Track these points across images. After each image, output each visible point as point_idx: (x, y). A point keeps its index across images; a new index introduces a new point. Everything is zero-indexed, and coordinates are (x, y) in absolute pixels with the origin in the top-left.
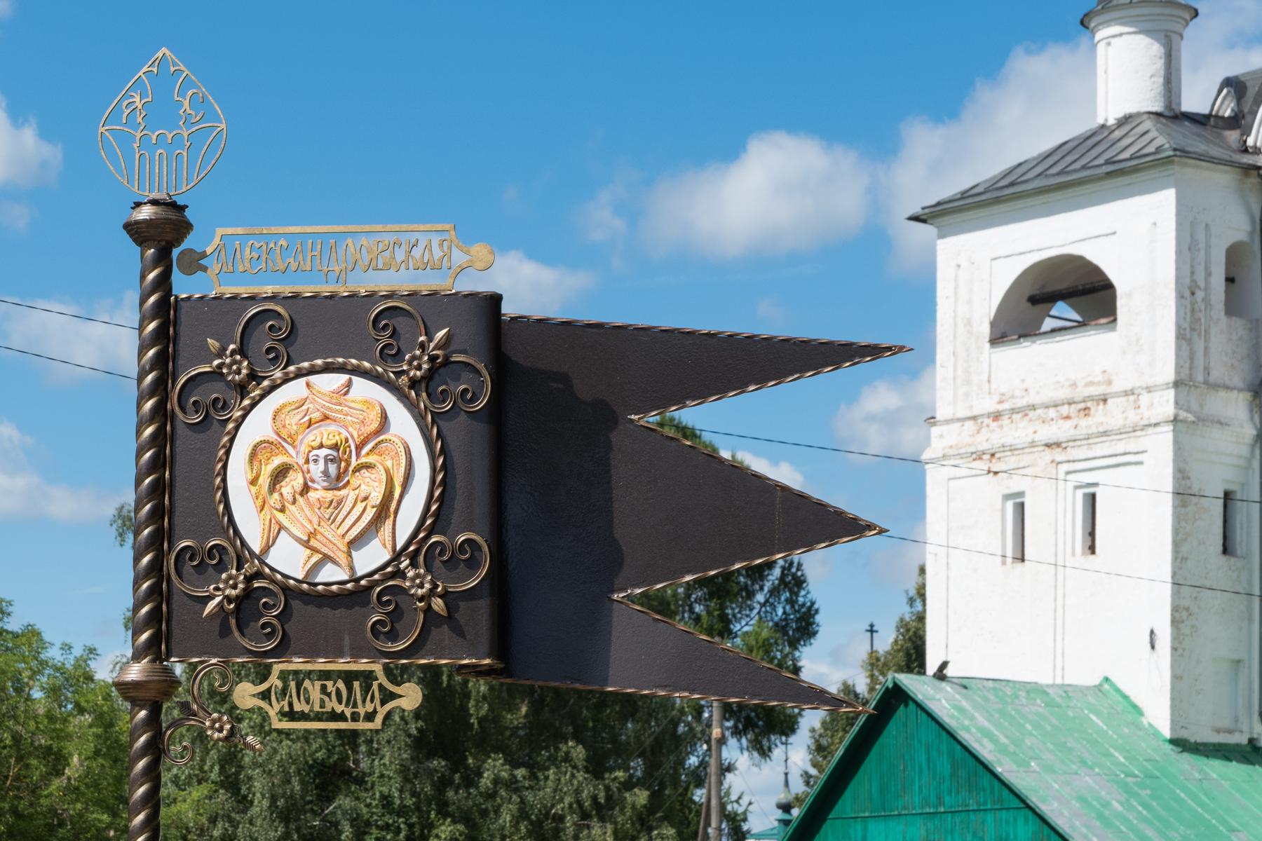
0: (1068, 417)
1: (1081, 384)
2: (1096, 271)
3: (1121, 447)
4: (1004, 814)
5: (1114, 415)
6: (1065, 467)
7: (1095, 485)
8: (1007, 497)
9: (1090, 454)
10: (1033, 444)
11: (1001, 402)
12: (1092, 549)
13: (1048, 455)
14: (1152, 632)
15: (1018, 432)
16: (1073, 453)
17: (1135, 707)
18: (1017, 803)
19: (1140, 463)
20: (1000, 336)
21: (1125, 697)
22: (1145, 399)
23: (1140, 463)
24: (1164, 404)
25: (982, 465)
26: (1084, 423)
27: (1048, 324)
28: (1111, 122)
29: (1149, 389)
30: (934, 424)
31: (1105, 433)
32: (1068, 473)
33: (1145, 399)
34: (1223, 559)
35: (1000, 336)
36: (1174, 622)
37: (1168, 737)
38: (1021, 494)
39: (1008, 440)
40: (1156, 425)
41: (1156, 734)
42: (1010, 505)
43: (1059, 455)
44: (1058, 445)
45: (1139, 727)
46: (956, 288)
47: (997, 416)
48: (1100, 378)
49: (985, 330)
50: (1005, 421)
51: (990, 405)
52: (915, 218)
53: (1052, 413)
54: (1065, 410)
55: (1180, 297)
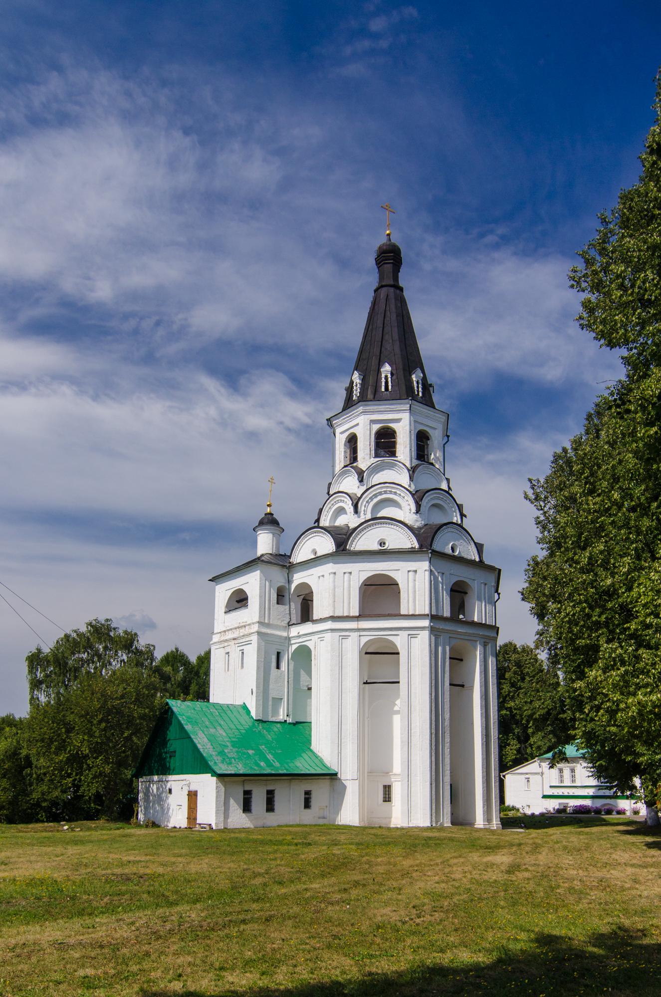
3: (247, 639)
7: (243, 650)
12: (242, 667)
13: (233, 642)
36: (257, 687)
43: (236, 642)
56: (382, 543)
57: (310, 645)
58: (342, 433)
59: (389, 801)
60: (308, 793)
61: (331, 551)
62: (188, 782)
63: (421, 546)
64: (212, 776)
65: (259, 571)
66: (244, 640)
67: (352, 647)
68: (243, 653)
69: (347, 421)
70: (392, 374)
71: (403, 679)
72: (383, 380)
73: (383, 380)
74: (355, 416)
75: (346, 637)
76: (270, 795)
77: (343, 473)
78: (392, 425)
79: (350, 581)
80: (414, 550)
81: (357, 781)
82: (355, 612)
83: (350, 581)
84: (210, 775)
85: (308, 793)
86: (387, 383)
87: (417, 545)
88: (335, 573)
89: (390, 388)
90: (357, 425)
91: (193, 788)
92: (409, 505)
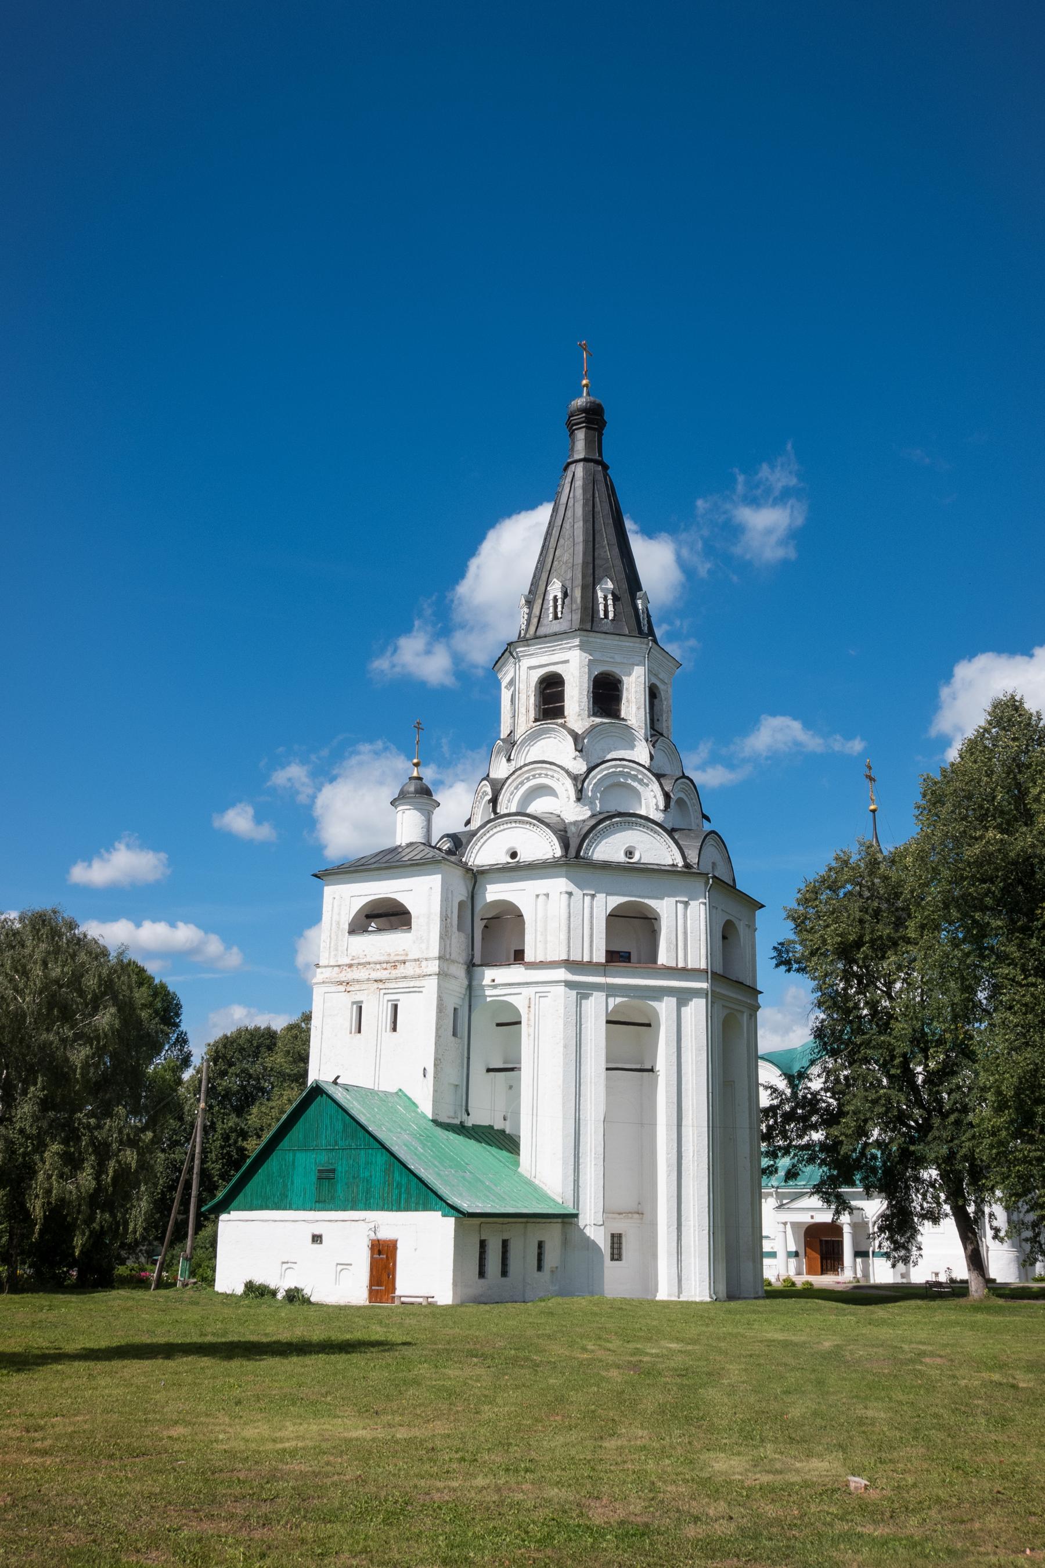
0: (386, 969)
1: (392, 955)
2: (402, 905)
3: (412, 984)
4: (370, 1151)
5: (409, 969)
6: (383, 991)
7: (398, 1000)
8: (354, 1003)
9: (397, 986)
10: (368, 980)
11: (352, 960)
12: (394, 1029)
13: (376, 985)
14: (425, 1069)
15: (362, 974)
16: (387, 985)
17: (414, 1103)
18: (377, 1145)
19: (421, 992)
20: (352, 931)
21: (409, 1099)
22: (424, 964)
23: (421, 992)
24: (434, 967)
25: (342, 988)
26: (394, 972)
27: (370, 929)
28: (403, 844)
29: (426, 959)
30: (319, 967)
31: (405, 977)
32: (385, 994)
33: (424, 964)
34: (453, 1038)
35: (352, 931)
36: (435, 1065)
37: (431, 1118)
38: (362, 1002)
39: (356, 977)
40: (430, 975)
41: (425, 1117)
42: (355, 1006)
43: (381, 985)
44: (381, 981)
45: (417, 1113)
46: (333, 907)
47: (350, 966)
48: (402, 953)
49: (346, 927)
50: (354, 968)
51: (348, 961)
52: (315, 876)
53: (378, 966)
54: (384, 965)
55: (442, 920)
56: (629, 853)
57: (519, 1002)
58: (530, 668)
59: (617, 1260)
60: (541, 1245)
61: (549, 855)
62: (372, 1225)
63: (687, 865)
64: (444, 1216)
65: (439, 876)
66: (401, 985)
67: (596, 1008)
68: (396, 1007)
69: (546, 652)
70: (613, 594)
71: (663, 1061)
72: (601, 600)
73: (601, 600)
74: (560, 649)
75: (586, 996)
76: (505, 1244)
77: (534, 737)
78: (616, 670)
79: (592, 908)
80: (674, 869)
81: (603, 1227)
82: (600, 957)
83: (592, 908)
84: (440, 1213)
85: (541, 1245)
86: (606, 606)
87: (681, 863)
88: (570, 894)
89: (611, 615)
90: (567, 662)
91: (384, 1235)
92: (655, 797)
